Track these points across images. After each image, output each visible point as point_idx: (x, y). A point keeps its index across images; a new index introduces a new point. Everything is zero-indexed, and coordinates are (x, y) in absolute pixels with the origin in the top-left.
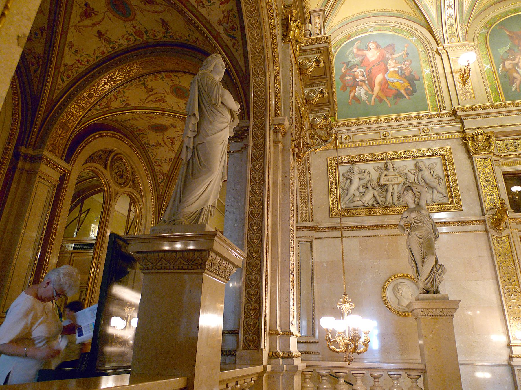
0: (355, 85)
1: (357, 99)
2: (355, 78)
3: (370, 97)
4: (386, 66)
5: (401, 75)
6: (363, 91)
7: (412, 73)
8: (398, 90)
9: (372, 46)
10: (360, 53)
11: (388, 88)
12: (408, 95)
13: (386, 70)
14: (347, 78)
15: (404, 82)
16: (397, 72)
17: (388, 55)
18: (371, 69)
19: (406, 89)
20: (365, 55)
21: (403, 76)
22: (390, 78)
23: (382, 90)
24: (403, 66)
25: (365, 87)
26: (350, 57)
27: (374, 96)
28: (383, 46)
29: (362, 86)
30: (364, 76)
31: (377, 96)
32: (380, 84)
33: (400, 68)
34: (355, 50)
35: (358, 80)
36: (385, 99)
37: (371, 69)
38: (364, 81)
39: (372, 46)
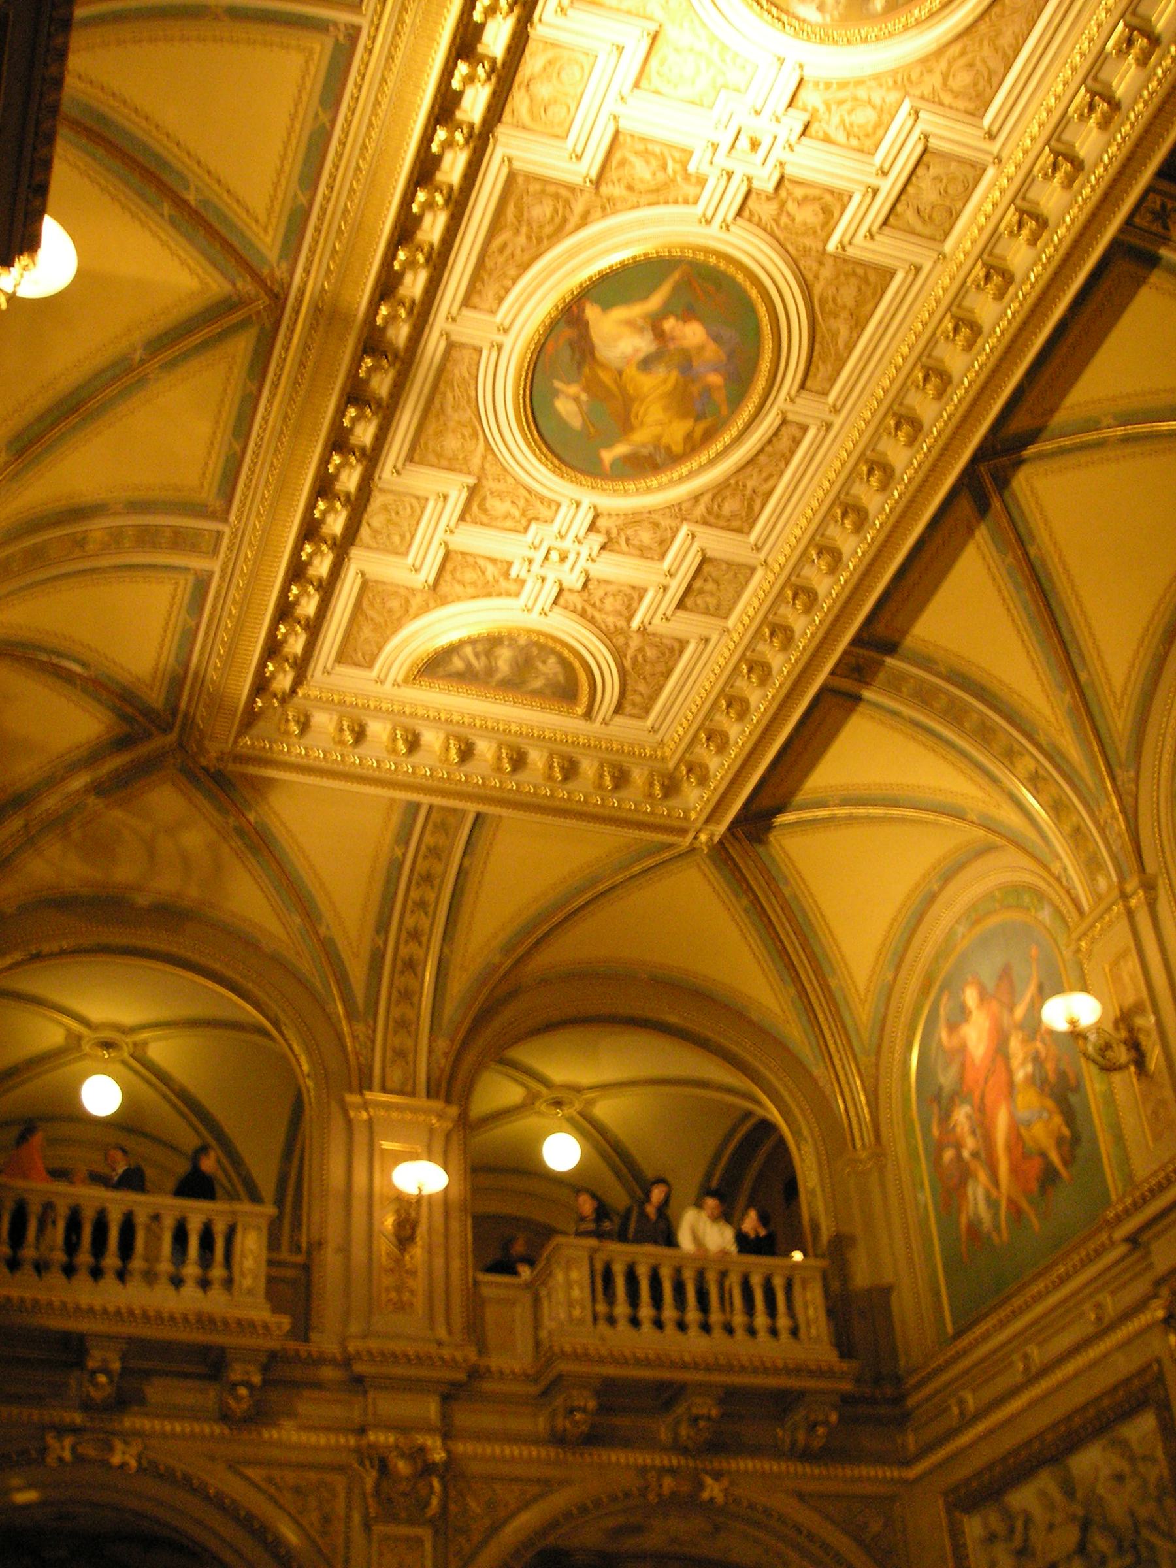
0: (964, 1175)
1: (974, 1229)
2: (958, 1146)
3: (996, 1215)
4: (1007, 1058)
5: (1043, 1091)
6: (980, 1192)
7: (1063, 1065)
8: (1043, 1155)
9: (971, 996)
10: (955, 1042)
11: (1026, 1156)
12: (1066, 1163)
13: (1011, 1084)
14: (948, 1155)
15: (1051, 1113)
16: (1030, 1080)
17: (1006, 1020)
18: (982, 1097)
19: (1060, 1141)
20: (963, 1049)
21: (1047, 1089)
22: (1023, 1113)
23: (1014, 1170)
24: (1039, 1045)
25: (983, 1176)
26: (939, 1070)
27: (1004, 1204)
28: (990, 986)
29: (976, 1177)
30: (973, 1133)
31: (1011, 1202)
32: (1009, 1149)
33: (1037, 1059)
34: (944, 1034)
35: (966, 1154)
36: (1025, 1205)
37: (982, 1097)
38: (975, 1155)
39: (971, 996)
